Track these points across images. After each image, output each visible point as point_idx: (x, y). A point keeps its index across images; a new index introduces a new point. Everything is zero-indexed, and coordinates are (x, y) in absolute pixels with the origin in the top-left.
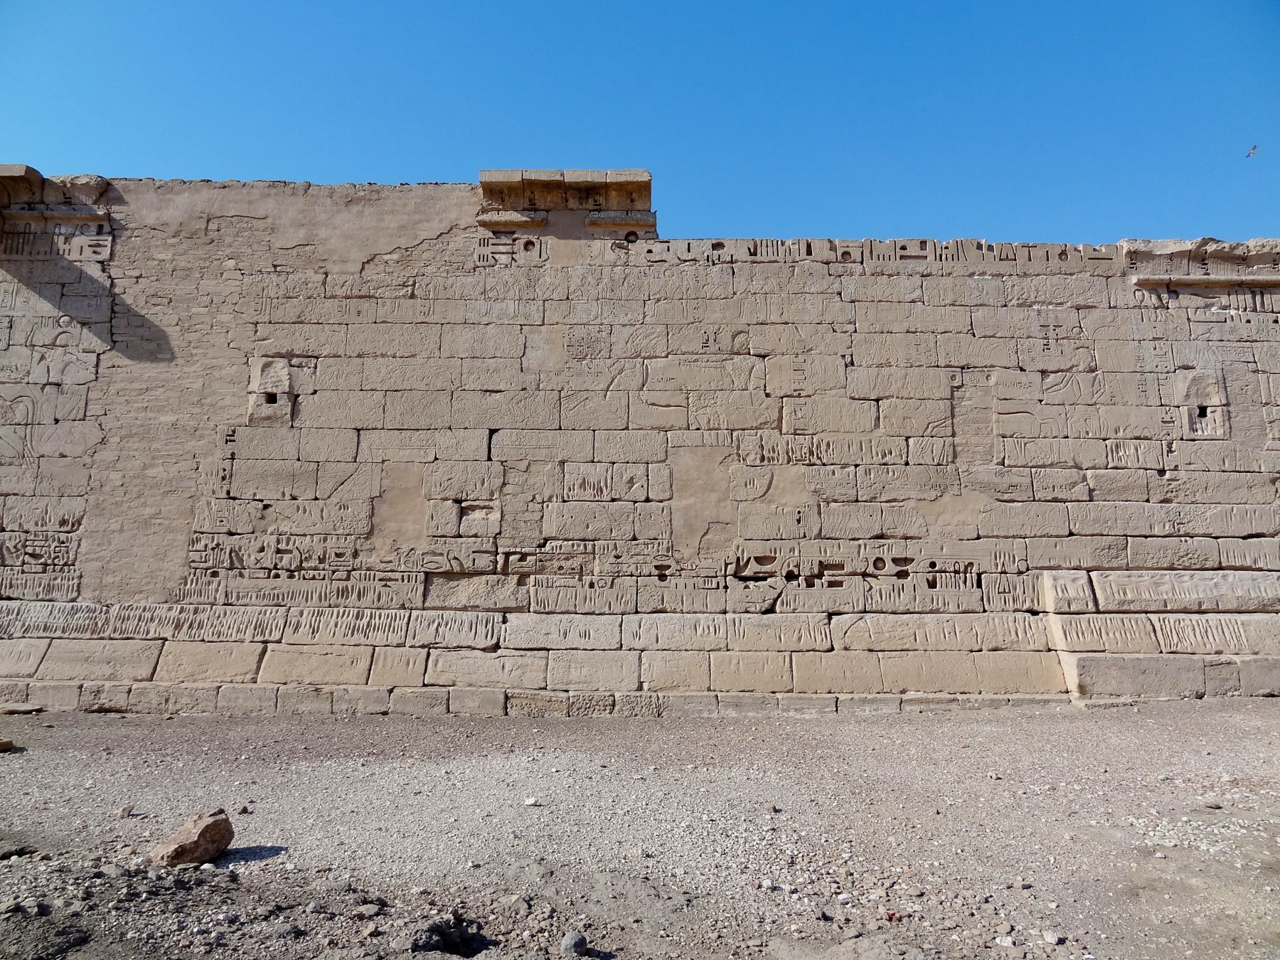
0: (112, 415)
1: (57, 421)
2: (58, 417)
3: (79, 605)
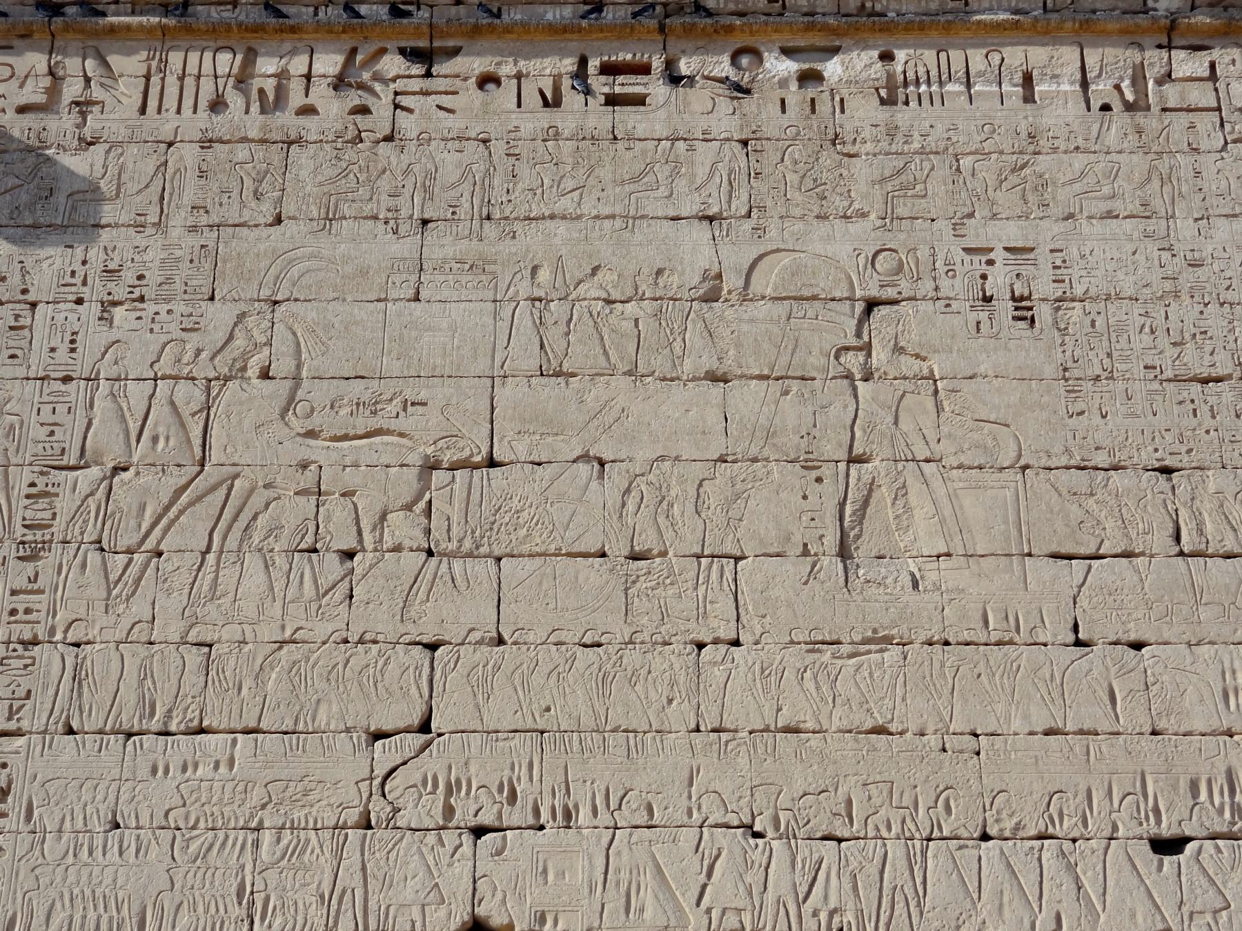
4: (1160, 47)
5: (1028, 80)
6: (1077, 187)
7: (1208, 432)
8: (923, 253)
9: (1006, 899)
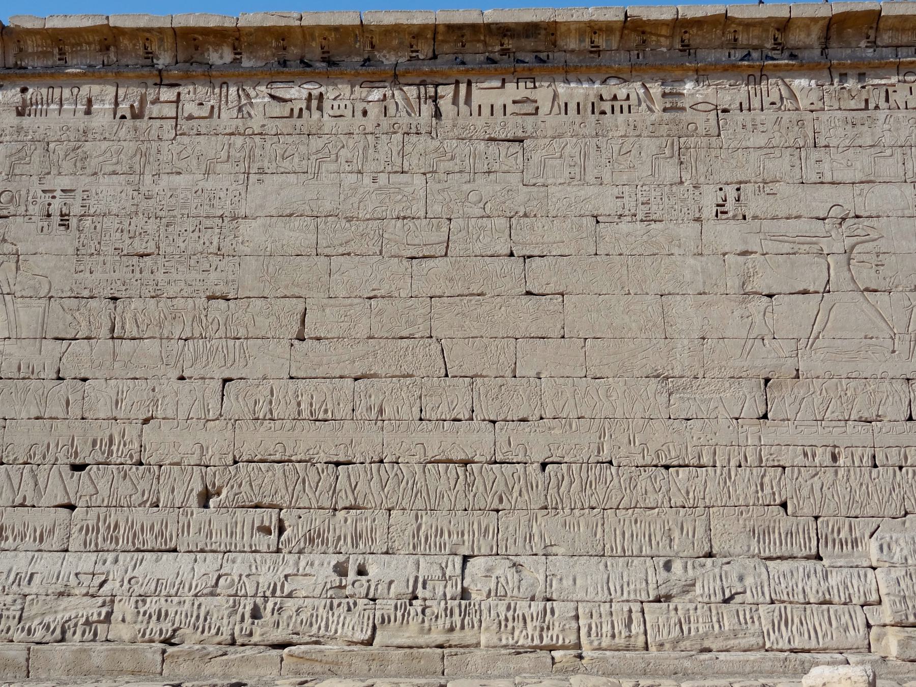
4: (156, 84)
5: (90, 102)
6: (101, 159)
7: (136, 280)
8: (23, 192)
9: (4, 489)
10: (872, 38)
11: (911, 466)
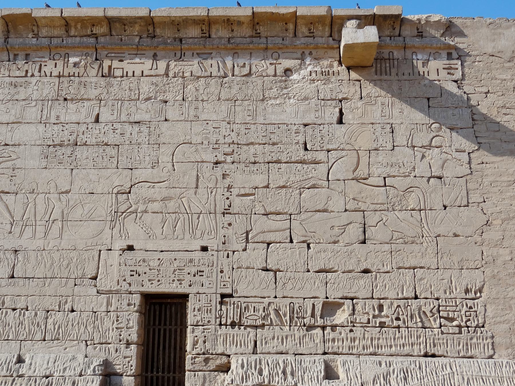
0: (490, 202)
1: (445, 207)
2: (446, 203)
3: (500, 360)
10: (36, 32)
11: (6, 308)
